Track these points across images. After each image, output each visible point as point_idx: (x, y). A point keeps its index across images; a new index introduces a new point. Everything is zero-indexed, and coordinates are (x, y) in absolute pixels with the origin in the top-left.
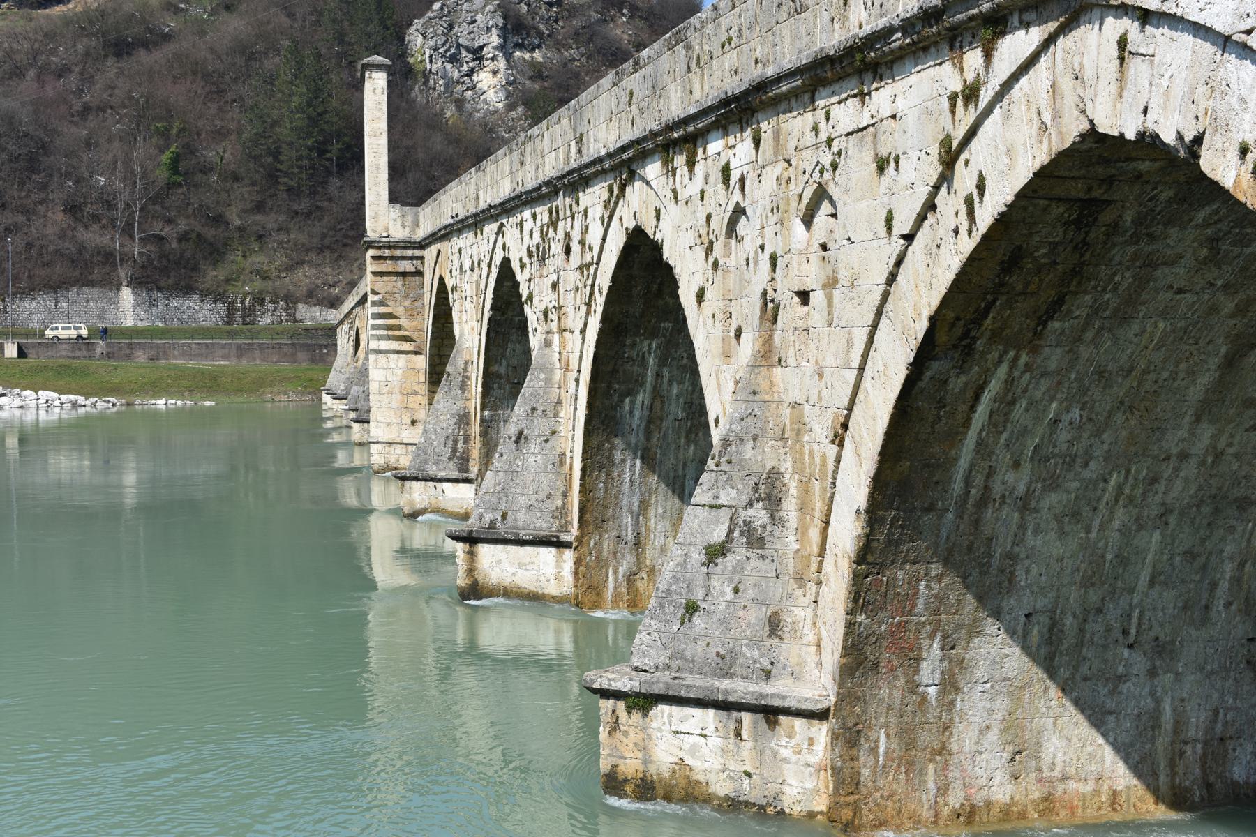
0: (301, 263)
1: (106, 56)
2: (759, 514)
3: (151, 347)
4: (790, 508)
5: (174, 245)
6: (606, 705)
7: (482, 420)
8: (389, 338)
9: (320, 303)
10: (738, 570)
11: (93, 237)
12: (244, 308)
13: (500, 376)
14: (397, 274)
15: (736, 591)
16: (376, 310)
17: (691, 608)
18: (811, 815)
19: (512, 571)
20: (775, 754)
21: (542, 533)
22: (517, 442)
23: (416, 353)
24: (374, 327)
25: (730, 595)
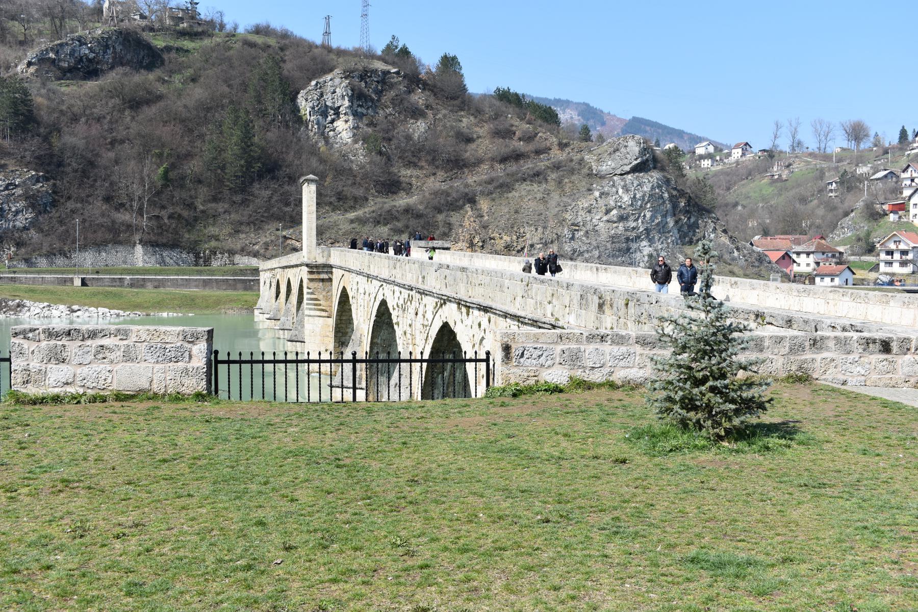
0: (237, 232)
1: (124, 109)
3: (155, 280)
5: (166, 221)
8: (315, 309)
9: (249, 254)
11: (124, 217)
12: (205, 257)
13: (378, 344)
16: (309, 296)
23: (328, 317)
24: (307, 304)
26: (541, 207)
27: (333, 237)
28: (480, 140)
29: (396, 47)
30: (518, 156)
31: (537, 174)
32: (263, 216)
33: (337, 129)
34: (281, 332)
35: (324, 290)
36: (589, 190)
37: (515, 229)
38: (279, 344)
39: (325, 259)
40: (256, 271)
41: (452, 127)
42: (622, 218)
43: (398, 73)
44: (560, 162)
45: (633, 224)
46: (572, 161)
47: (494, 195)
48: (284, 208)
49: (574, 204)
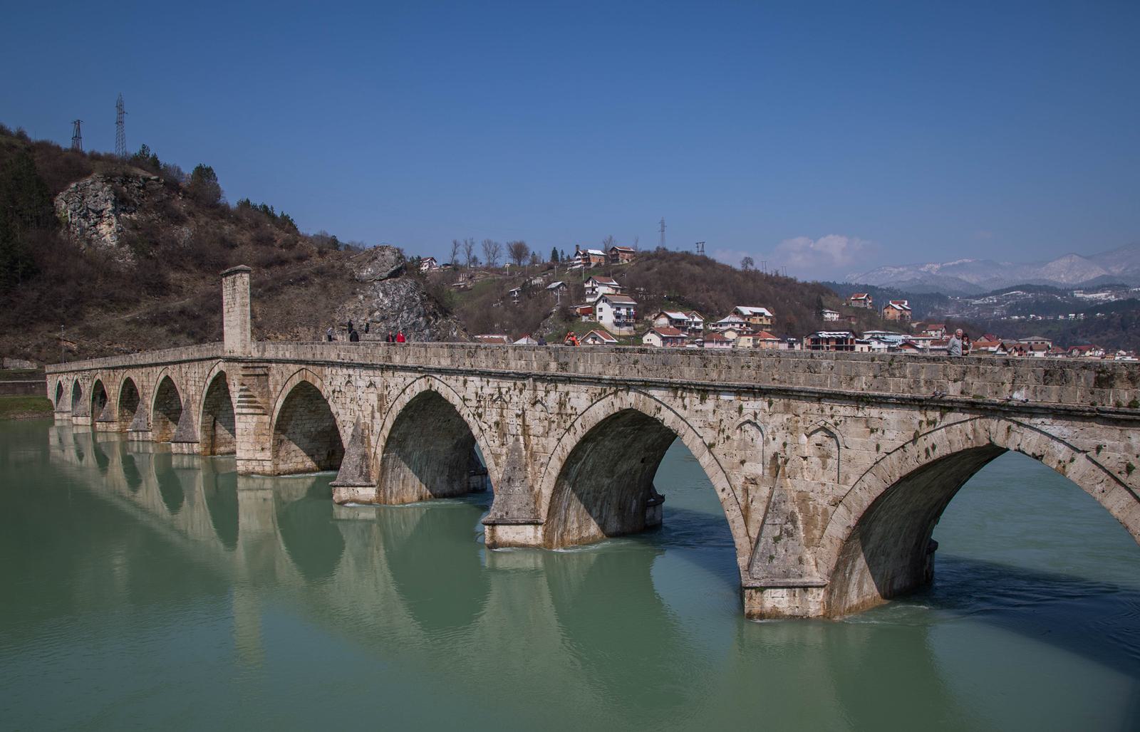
2: (790, 526)
4: (800, 525)
6: (747, 592)
7: (383, 458)
8: (248, 407)
10: (786, 544)
13: (394, 438)
14: (255, 375)
15: (786, 551)
16: (242, 393)
17: (772, 558)
18: (818, 616)
19: (512, 536)
20: (807, 600)
21: (529, 520)
22: (508, 482)
23: (264, 414)
24: (239, 402)
25: (784, 552)
26: (311, 309)
27: (110, 339)
28: (244, 247)
29: (148, 155)
30: (282, 262)
31: (304, 278)
32: (32, 318)
33: (100, 232)
34: (135, 434)
35: (259, 386)
36: (353, 294)
37: (289, 329)
38: (132, 447)
39: (260, 353)
40: (40, 375)
41: (215, 234)
42: (383, 319)
43: (157, 180)
44: (322, 268)
45: (392, 324)
46: (333, 267)
47: (265, 298)
48: (54, 310)
49: (341, 306)
